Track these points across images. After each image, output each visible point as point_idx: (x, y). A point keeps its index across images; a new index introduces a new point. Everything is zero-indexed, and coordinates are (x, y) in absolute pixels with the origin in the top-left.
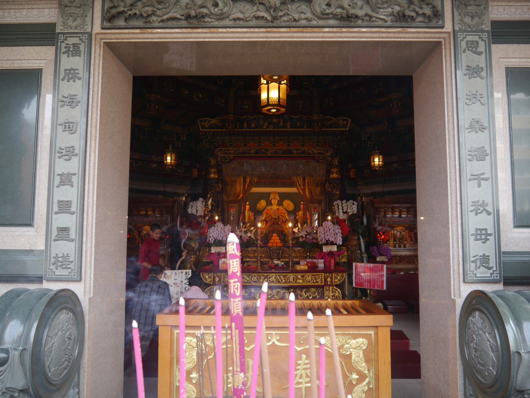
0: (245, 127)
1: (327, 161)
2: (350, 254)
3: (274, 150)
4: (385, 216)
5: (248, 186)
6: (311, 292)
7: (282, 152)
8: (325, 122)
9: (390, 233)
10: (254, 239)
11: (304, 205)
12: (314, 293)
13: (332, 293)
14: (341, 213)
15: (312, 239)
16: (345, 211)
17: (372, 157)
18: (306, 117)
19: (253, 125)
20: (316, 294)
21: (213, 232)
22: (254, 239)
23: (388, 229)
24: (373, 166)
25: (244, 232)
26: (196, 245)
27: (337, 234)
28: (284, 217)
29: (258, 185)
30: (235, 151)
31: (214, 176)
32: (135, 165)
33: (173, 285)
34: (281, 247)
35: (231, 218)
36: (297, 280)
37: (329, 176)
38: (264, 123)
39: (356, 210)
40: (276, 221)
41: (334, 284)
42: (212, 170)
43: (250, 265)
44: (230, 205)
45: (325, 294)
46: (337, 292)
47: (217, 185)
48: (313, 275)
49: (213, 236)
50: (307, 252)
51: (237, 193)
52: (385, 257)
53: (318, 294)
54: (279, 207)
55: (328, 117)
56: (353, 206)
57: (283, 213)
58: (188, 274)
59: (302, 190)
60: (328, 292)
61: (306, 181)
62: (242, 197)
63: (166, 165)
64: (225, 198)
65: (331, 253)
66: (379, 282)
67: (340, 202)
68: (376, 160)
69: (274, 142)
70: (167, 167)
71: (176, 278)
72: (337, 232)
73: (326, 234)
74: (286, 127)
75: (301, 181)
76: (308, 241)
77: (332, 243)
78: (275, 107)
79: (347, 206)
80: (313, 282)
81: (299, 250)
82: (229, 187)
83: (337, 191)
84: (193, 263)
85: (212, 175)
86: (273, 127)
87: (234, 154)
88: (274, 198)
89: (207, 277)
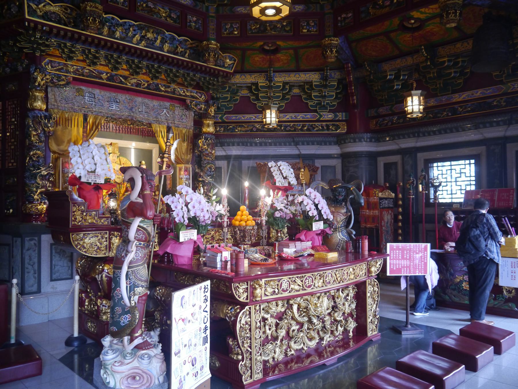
0: (105, 33)
7: (146, 85)
19: (118, 34)
38: (135, 35)
51: (73, 140)
66: (421, 266)
86: (145, 44)
87: (74, 73)
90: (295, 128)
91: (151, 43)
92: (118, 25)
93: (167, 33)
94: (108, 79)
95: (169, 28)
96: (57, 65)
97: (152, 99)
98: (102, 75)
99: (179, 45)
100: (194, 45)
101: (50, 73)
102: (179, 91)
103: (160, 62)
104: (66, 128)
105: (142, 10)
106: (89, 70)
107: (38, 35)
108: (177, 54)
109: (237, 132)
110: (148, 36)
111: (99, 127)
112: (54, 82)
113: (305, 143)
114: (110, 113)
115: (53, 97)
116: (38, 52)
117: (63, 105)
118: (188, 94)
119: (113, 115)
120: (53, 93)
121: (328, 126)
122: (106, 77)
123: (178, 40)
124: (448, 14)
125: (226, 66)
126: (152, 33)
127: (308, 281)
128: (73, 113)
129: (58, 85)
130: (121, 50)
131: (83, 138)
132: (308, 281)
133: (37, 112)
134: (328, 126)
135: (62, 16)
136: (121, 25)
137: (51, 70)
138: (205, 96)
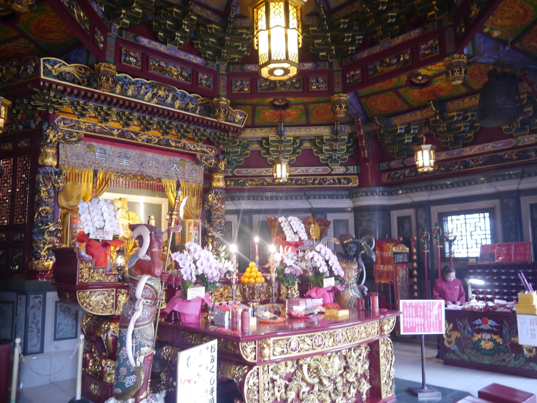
7: (157, 141)
19: (130, 92)
38: (147, 93)
51: (82, 196)
66: (436, 324)
74: (172, 106)
86: (157, 102)
87: (86, 129)
90: (306, 182)
91: (162, 101)
92: (130, 83)
93: (178, 91)
94: (119, 135)
95: (180, 86)
96: (69, 122)
97: (163, 154)
98: (113, 132)
100: (204, 102)
103: (170, 118)
104: (76, 184)
105: (154, 69)
107: (52, 94)
108: (187, 110)
111: (109, 182)
113: (317, 197)
115: (64, 153)
117: (73, 161)
118: (198, 149)
119: (124, 170)
120: (64, 149)
121: (339, 180)
122: (117, 133)
123: (189, 97)
124: (453, 72)
126: (164, 90)
129: (70, 141)
130: (132, 107)
134: (339, 180)
135: (76, 75)
138: (215, 150)
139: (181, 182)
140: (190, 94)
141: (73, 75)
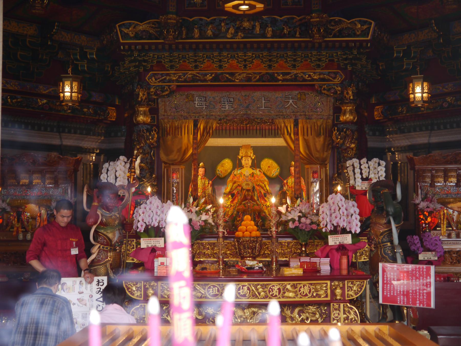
0: (197, 36)
1: (335, 93)
2: (373, 249)
3: (245, 75)
4: (432, 185)
5: (202, 135)
6: (309, 313)
8: (332, 27)
9: (442, 213)
10: (213, 224)
11: (295, 167)
12: (314, 314)
13: (344, 313)
14: (359, 180)
15: (310, 224)
16: (364, 177)
17: (411, 85)
18: (298, 18)
19: (209, 33)
20: (317, 316)
21: (143, 213)
22: (213, 224)
23: (439, 206)
24: (412, 100)
25: (196, 212)
26: (114, 235)
27: (352, 215)
28: (263, 188)
29: (219, 133)
30: (180, 77)
31: (145, 119)
32: (9, 100)
33: (76, 302)
34: (257, 237)
35: (173, 190)
36: (284, 293)
37: (338, 118)
38: (229, 29)
39: (384, 175)
40: (248, 195)
41: (347, 299)
42: (141, 109)
43: (205, 268)
44: (172, 167)
45: (332, 316)
46: (352, 313)
47: (150, 134)
48: (311, 284)
49: (143, 220)
50: (302, 245)
51: (183, 148)
52: (434, 253)
53: (321, 315)
54: (254, 171)
55: (337, 18)
56: (379, 168)
57: (261, 181)
58: (102, 284)
59: (293, 142)
60: (338, 312)
61: (300, 126)
62: (192, 154)
63: (63, 101)
64: (163, 157)
65: (342, 248)
66: (423, 296)
67: (358, 161)
68: (418, 89)
69: (245, 60)
70: (64, 104)
71: (81, 290)
72: (352, 211)
73: (334, 215)
74: (264, 36)
75: (291, 127)
76: (304, 228)
77: (344, 231)
78: (246, 2)
79: (369, 167)
80: (313, 296)
81: (289, 243)
82: (169, 137)
83: (351, 143)
84: (111, 265)
85: (141, 118)
86: (243, 35)
87: (177, 81)
88: (246, 156)
89: (134, 289)
92: (208, 24)
96: (160, 76)
98: (206, 77)
99: (284, 25)
101: (154, 85)
102: (302, 76)
106: (192, 74)
107: (136, 54)
108: (284, 36)
109: (423, 111)
110: (244, 26)
112: (158, 94)
114: (223, 114)
115: (163, 107)
116: (141, 68)
117: (173, 114)
118: (315, 77)
119: (226, 116)
120: (163, 103)
122: (211, 78)
125: (358, 33)
126: (248, 21)
127: (213, 290)
128: (183, 120)
129: (162, 96)
130: (221, 47)
131: (193, 145)
132: (213, 290)
133: (140, 126)
136: (212, 23)
137: (154, 83)
139: (300, 121)
140: (281, 17)
141: (148, 31)
